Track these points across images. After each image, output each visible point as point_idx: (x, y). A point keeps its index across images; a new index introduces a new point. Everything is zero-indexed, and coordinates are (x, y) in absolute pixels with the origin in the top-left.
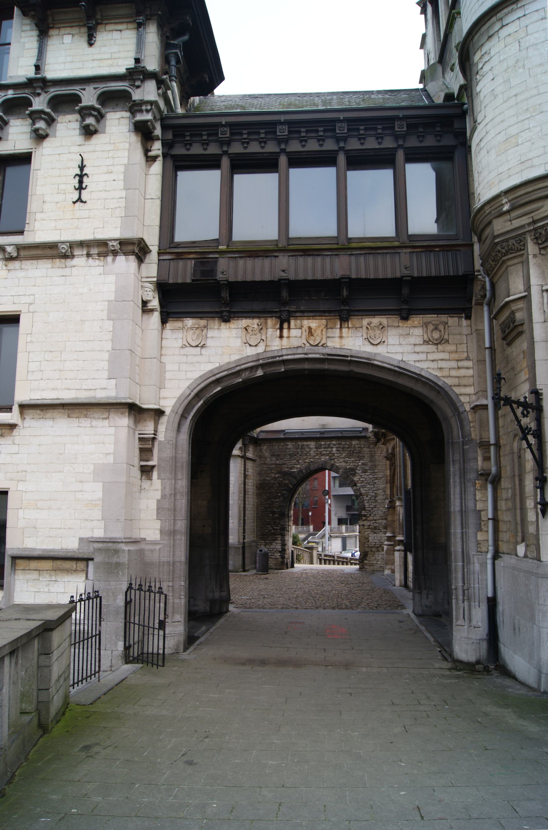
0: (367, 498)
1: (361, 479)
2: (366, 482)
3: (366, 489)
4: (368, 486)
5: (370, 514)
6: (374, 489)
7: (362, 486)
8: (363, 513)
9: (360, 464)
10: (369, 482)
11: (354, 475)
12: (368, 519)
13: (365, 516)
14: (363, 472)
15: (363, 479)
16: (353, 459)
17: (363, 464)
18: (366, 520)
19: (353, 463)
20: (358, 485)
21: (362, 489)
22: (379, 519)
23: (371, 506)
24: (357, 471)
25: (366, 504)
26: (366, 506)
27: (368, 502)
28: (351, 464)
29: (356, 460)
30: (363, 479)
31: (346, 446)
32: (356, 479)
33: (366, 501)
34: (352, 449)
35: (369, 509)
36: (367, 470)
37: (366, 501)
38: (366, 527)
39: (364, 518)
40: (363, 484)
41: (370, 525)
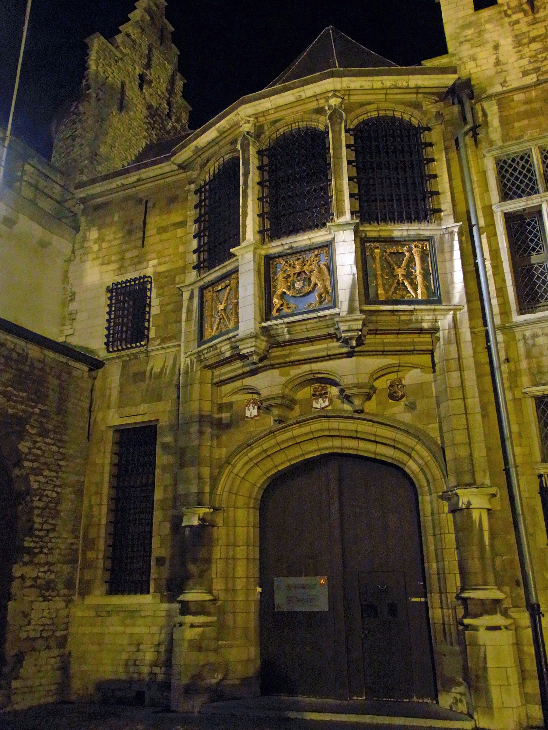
0: (41, 504)
1: (35, 451)
2: (42, 460)
3: (40, 478)
4: (47, 473)
5: (41, 548)
6: (58, 483)
7: (32, 468)
8: (26, 544)
9: (37, 411)
10: (50, 461)
11: (21, 435)
12: (36, 560)
13: (29, 551)
14: (39, 435)
15: (39, 452)
16: (25, 395)
17: (43, 414)
18: (30, 562)
19: (22, 403)
20: (26, 464)
21: (32, 478)
22: (59, 562)
23: (46, 526)
24: (28, 427)
25: (38, 520)
26: (37, 526)
27: (39, 516)
28: (19, 406)
29: (29, 399)
30: (39, 452)
31: (14, 356)
32: (24, 447)
33: (36, 512)
34: (26, 369)
35: (41, 533)
36: (48, 430)
37: (36, 512)
38: (28, 583)
39: (26, 558)
40: (36, 465)
41: (37, 577)
